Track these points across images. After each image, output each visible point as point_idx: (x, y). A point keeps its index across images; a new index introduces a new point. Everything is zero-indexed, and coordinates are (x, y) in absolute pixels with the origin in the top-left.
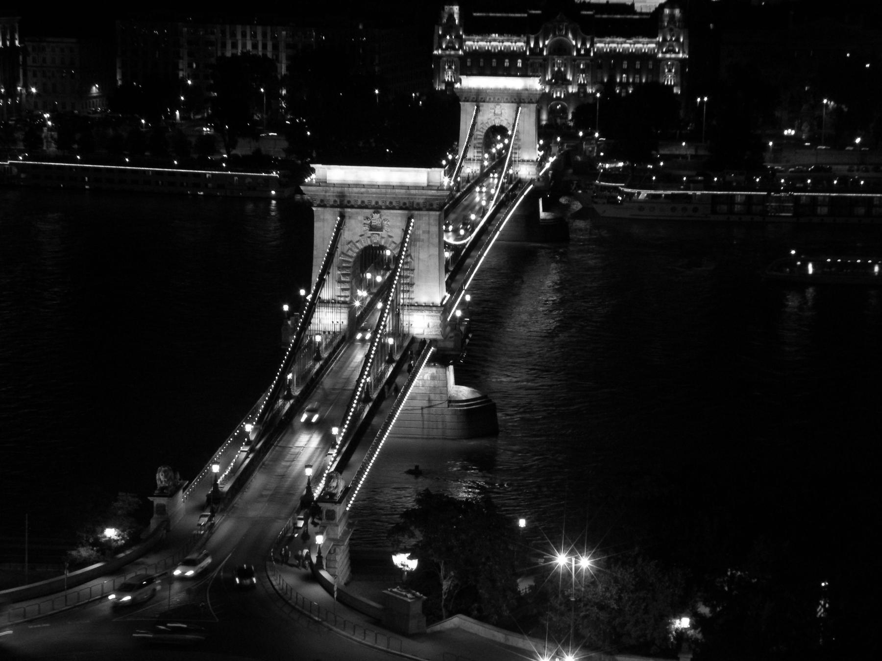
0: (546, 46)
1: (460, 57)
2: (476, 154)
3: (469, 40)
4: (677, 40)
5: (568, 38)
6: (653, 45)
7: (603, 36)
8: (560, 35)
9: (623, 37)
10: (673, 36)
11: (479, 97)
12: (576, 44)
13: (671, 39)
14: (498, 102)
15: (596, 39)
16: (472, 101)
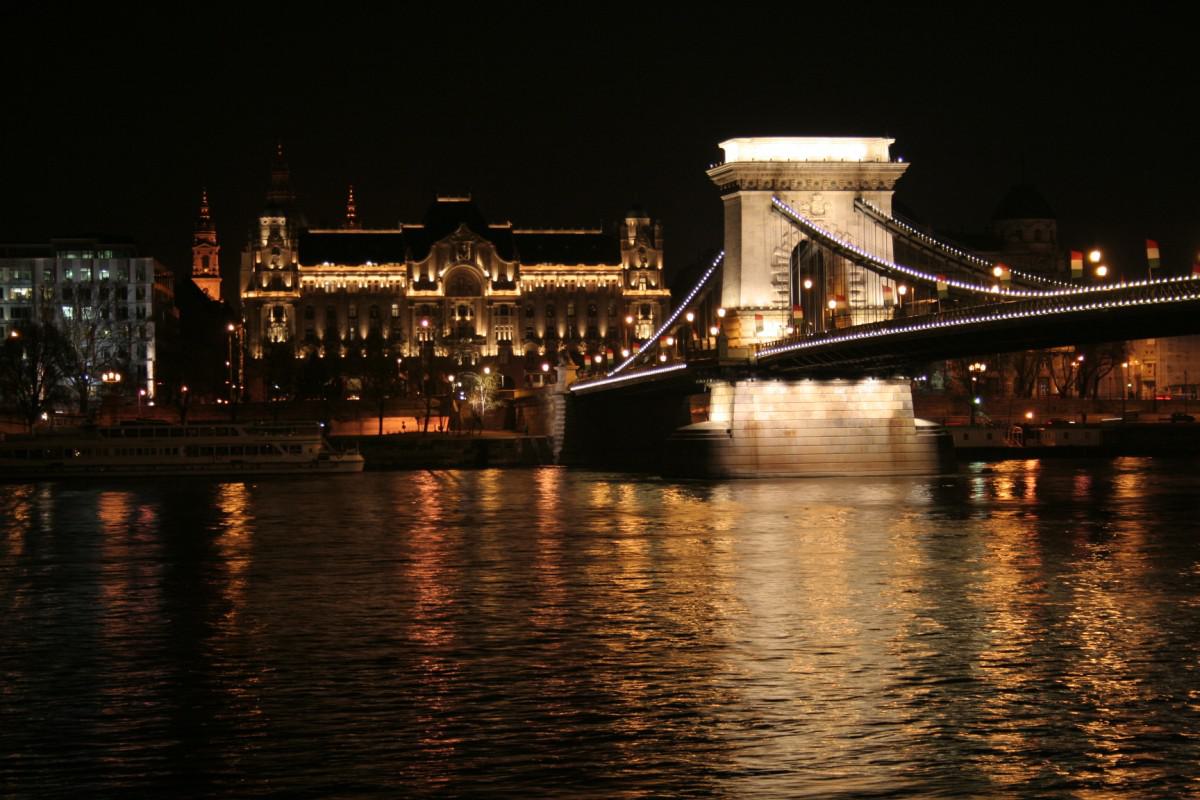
0: (441, 280)
1: (295, 302)
2: (779, 298)
3: (309, 273)
4: (653, 268)
5: (477, 266)
6: (615, 277)
7: (533, 263)
8: (464, 262)
9: (567, 263)
10: (646, 261)
11: (777, 180)
12: (491, 276)
13: (643, 267)
14: (817, 188)
15: (522, 268)
16: (765, 189)
